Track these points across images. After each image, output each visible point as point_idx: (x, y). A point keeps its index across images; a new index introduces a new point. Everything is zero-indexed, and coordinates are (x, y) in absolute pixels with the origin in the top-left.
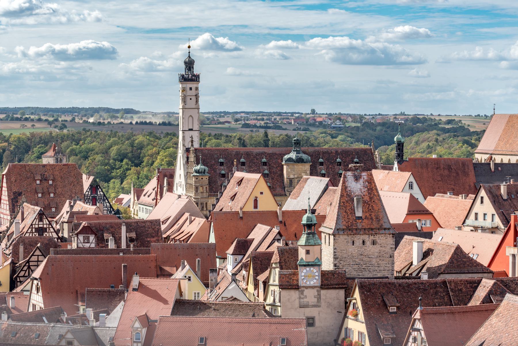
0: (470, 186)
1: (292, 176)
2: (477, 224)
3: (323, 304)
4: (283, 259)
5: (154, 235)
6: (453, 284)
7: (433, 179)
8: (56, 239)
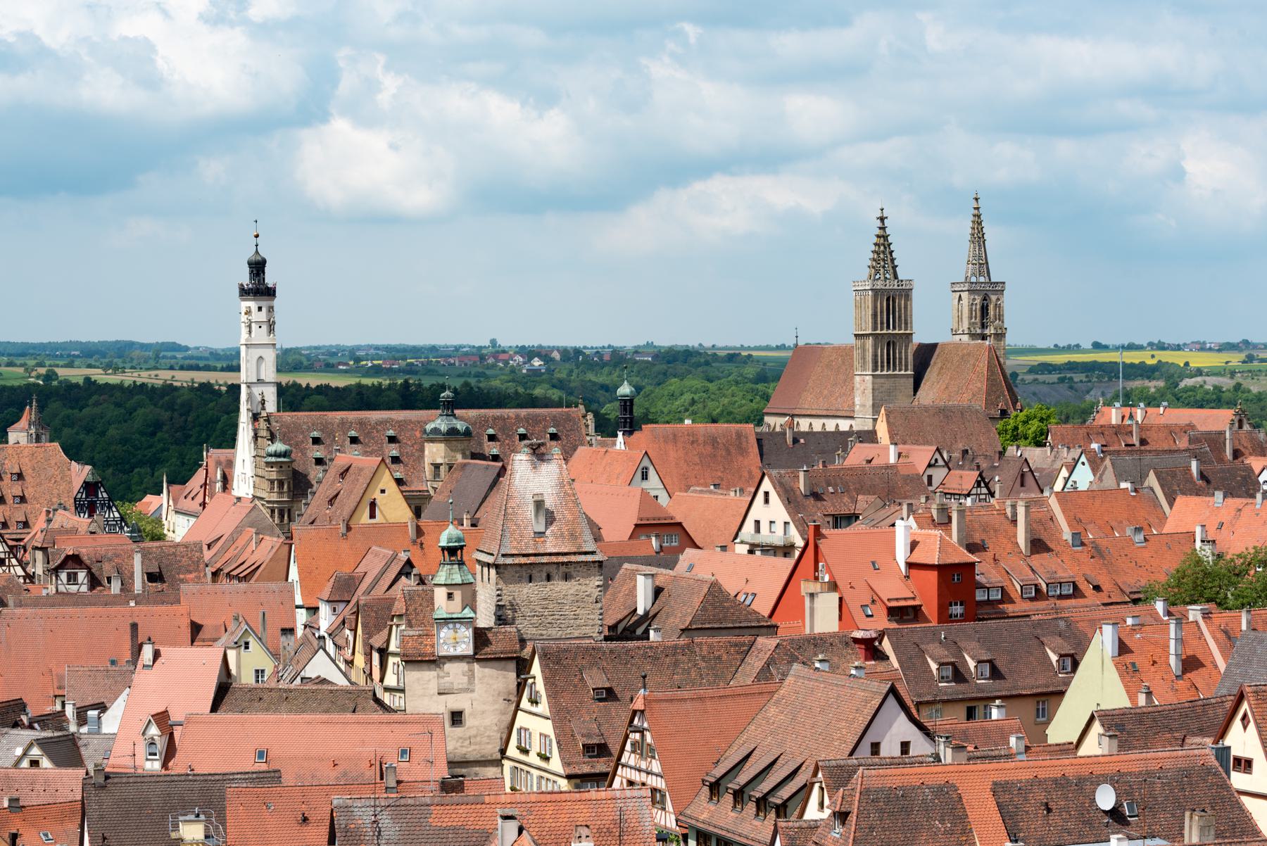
0: (750, 472)
1: (439, 461)
2: (759, 539)
3: (478, 686)
4: (411, 608)
6: (705, 648)
8: (21, 580)
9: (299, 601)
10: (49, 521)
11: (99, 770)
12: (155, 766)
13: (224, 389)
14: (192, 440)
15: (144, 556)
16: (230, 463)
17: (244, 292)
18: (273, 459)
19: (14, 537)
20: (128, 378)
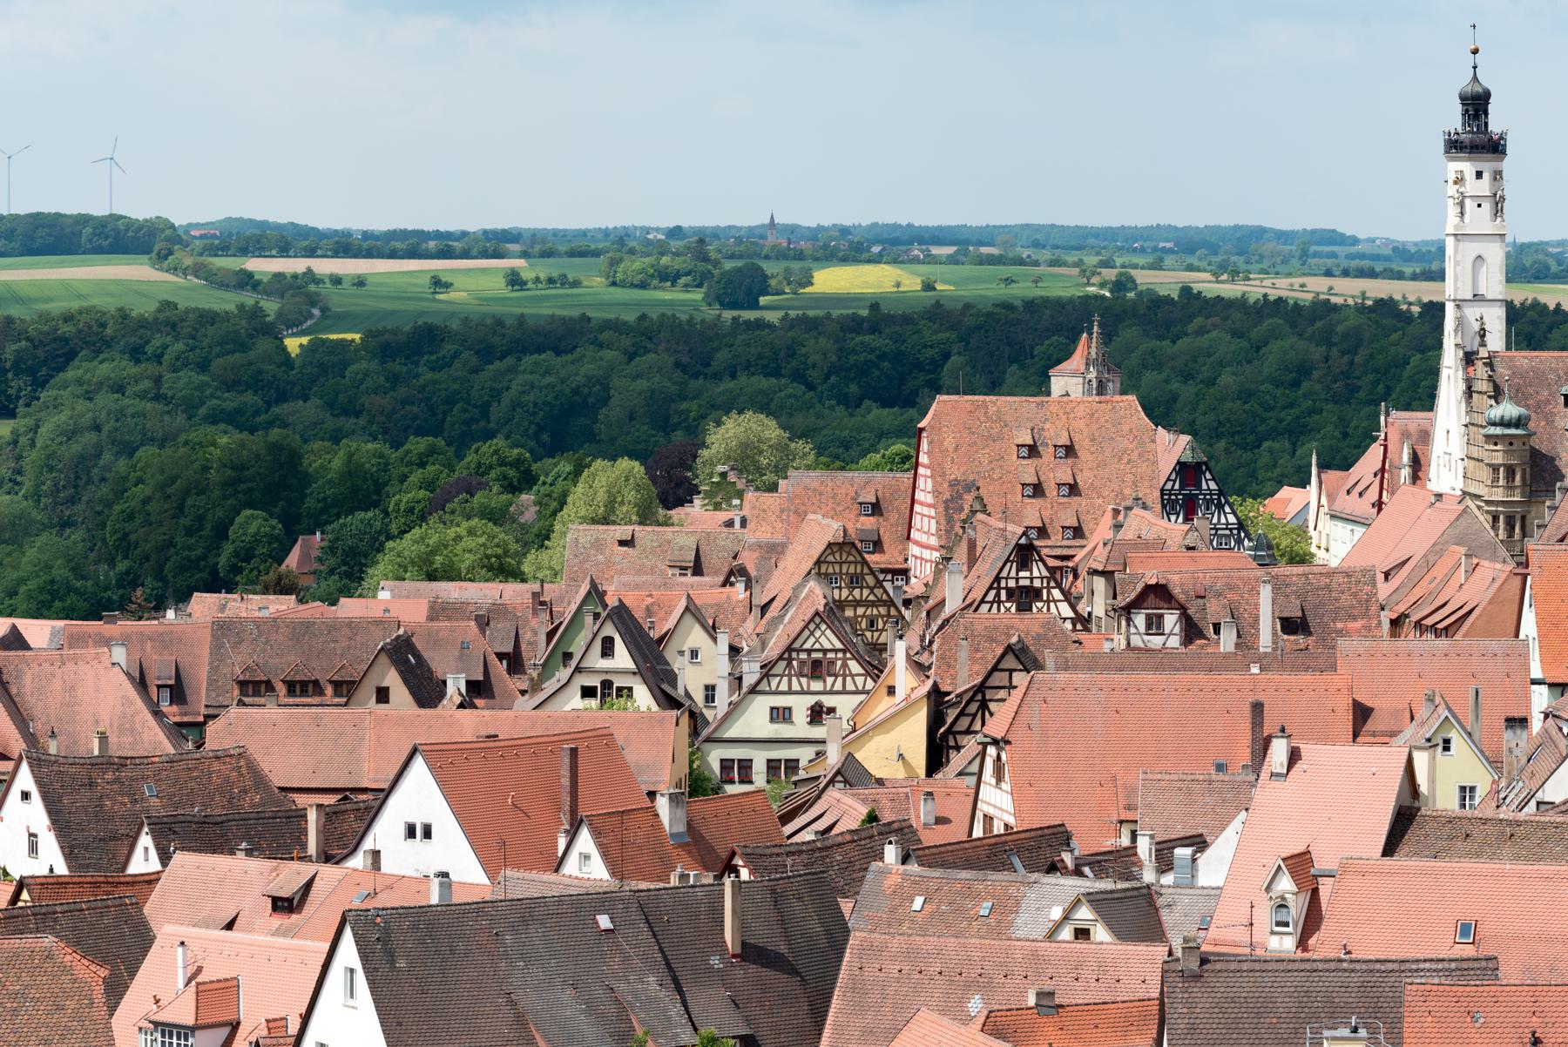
5: (1356, 612)
8: (1069, 625)
9: (1536, 672)
10: (1118, 527)
11: (1190, 948)
12: (1285, 944)
13: (1416, 309)
14: (1362, 395)
15: (1276, 590)
16: (1425, 436)
17: (1455, 146)
18: (1498, 431)
19: (1058, 552)
20: (1256, 288)
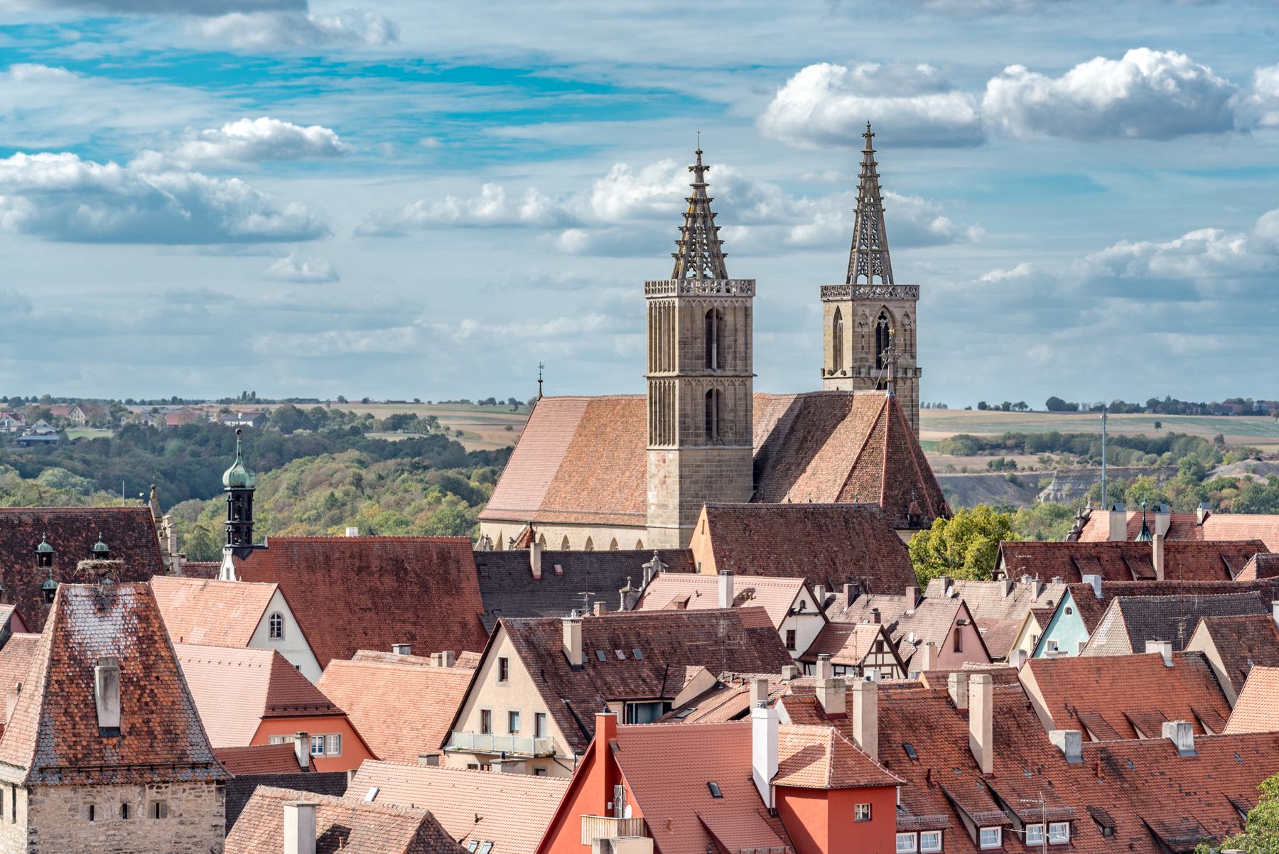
0: (464, 625)
2: (486, 744)
7: (347, 604)
